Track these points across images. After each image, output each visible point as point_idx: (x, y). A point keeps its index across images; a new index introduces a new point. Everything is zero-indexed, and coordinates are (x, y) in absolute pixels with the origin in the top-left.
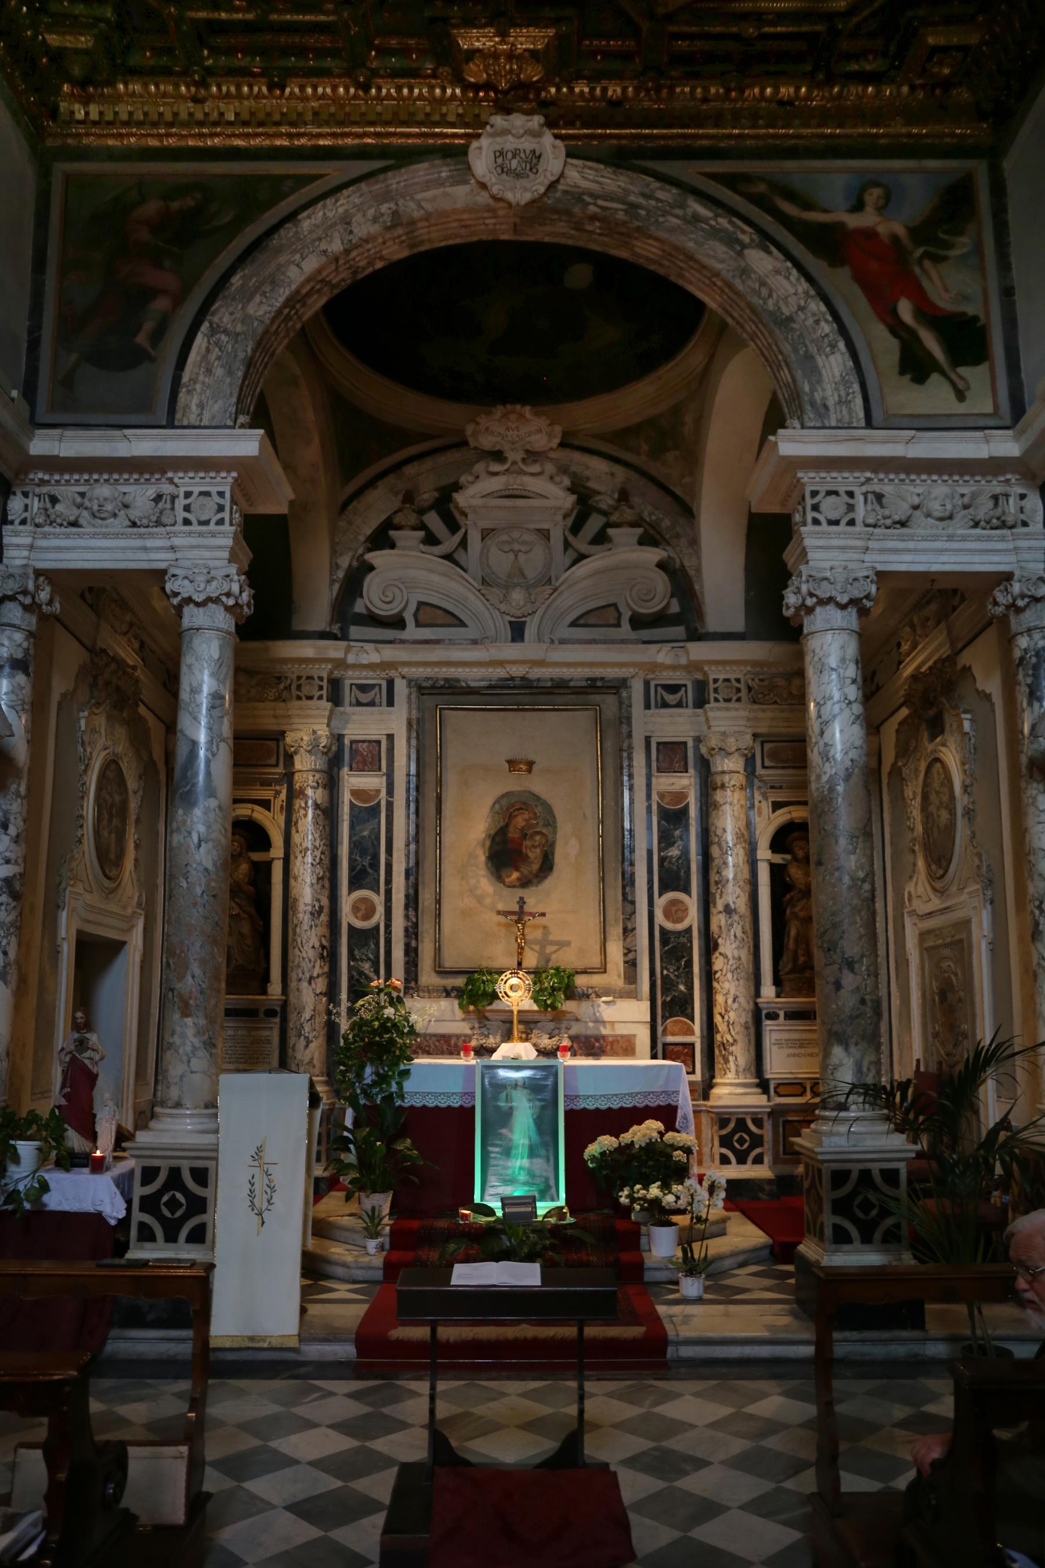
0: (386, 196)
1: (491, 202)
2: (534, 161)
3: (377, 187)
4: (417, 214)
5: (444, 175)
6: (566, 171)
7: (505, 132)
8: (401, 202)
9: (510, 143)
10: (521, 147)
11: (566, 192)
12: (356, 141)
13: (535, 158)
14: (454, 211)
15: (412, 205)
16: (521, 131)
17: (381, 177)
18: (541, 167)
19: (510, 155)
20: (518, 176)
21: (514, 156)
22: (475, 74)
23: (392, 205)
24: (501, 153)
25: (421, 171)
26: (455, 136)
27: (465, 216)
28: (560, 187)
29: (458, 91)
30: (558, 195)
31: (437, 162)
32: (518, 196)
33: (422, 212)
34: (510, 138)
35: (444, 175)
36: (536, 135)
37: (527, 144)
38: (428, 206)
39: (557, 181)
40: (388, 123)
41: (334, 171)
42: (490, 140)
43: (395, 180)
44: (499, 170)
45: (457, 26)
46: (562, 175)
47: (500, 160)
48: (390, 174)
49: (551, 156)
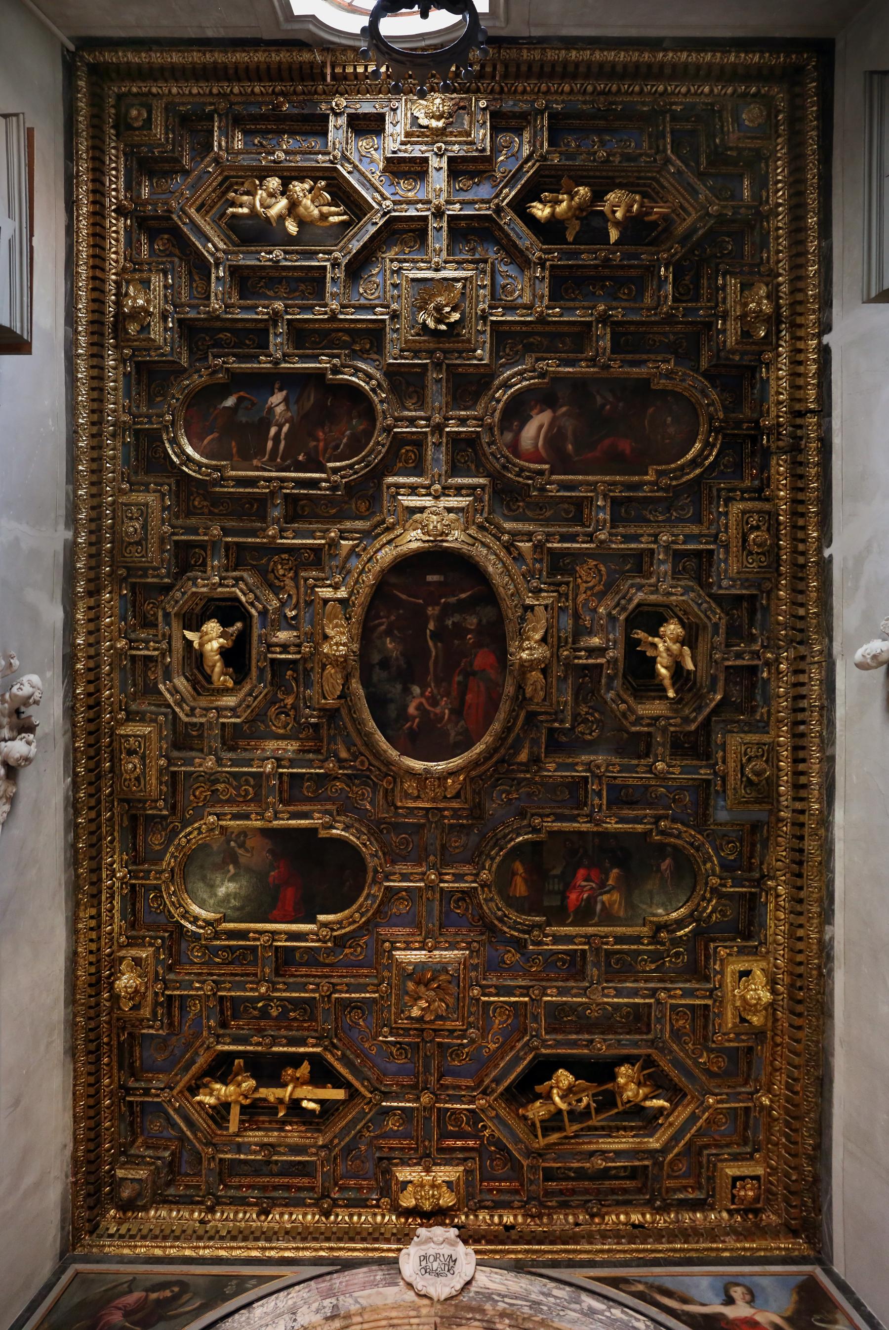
0: (330, 1293)
1: (416, 1299)
2: (452, 1264)
3: (323, 1285)
4: (354, 1308)
5: (378, 1278)
6: (477, 1276)
7: (430, 1240)
8: (341, 1298)
9: (431, 1249)
10: (441, 1252)
11: (477, 1293)
12: (314, 1254)
13: (453, 1260)
14: (386, 1307)
15: (350, 1301)
16: (441, 1239)
17: (328, 1278)
18: (457, 1269)
19: (432, 1258)
20: (438, 1275)
21: (435, 1260)
22: (408, 1201)
23: (334, 1300)
24: (425, 1257)
25: (360, 1274)
26: (389, 1250)
27: (394, 1314)
28: (473, 1288)
29: (394, 1218)
30: (472, 1294)
31: (374, 1268)
32: (439, 1290)
33: (358, 1306)
34: (432, 1245)
35: (378, 1278)
36: (453, 1244)
37: (446, 1250)
38: (364, 1302)
39: (469, 1283)
40: (340, 1240)
41: (290, 1273)
42: (417, 1248)
43: (339, 1280)
44: (423, 1271)
45: (396, 1165)
46: (473, 1278)
47: (424, 1263)
48: (335, 1275)
49: (464, 1262)
